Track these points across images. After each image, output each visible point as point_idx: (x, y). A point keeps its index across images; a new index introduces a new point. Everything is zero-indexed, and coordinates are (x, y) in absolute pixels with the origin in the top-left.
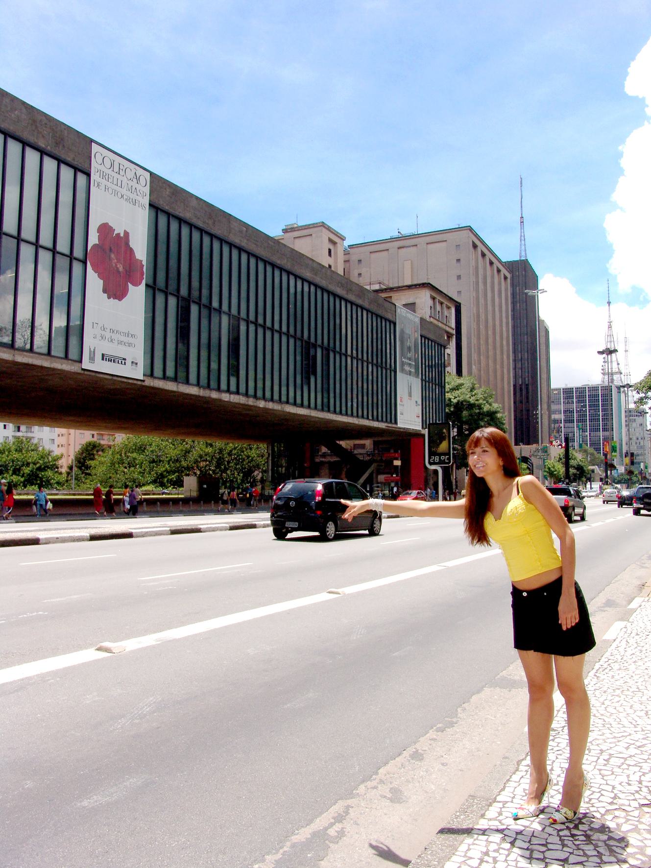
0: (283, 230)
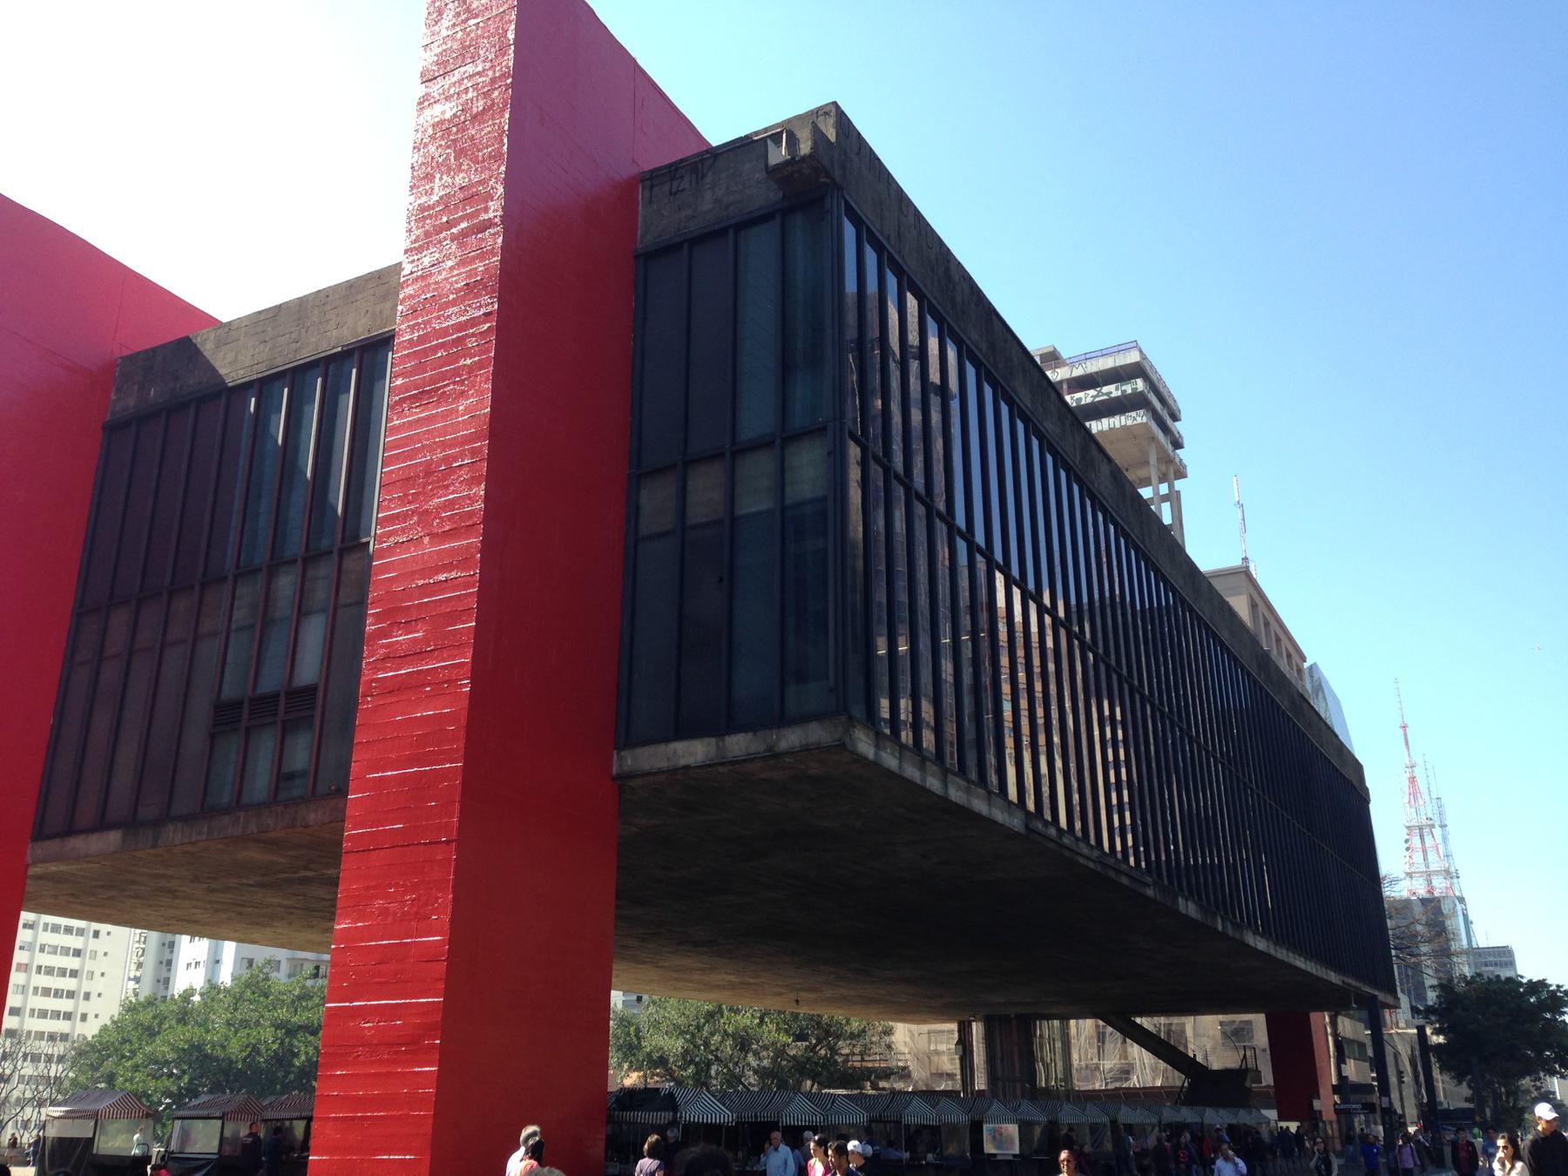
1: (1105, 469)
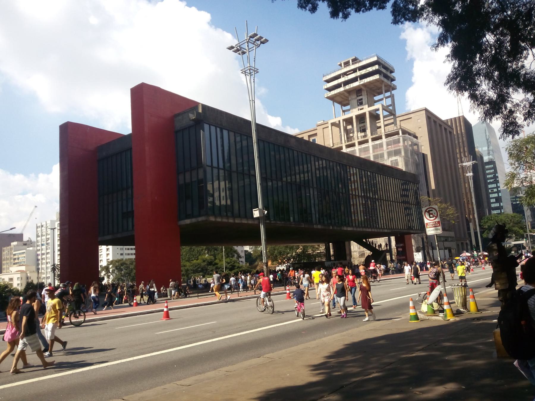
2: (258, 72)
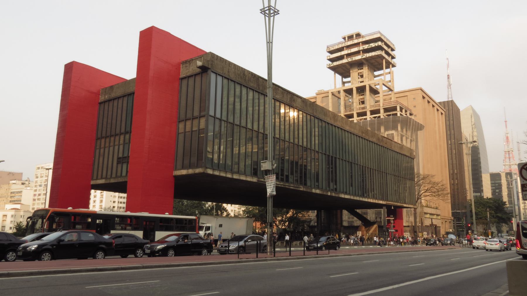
0: (316, 93)
1: (299, 100)
2: (278, 14)
